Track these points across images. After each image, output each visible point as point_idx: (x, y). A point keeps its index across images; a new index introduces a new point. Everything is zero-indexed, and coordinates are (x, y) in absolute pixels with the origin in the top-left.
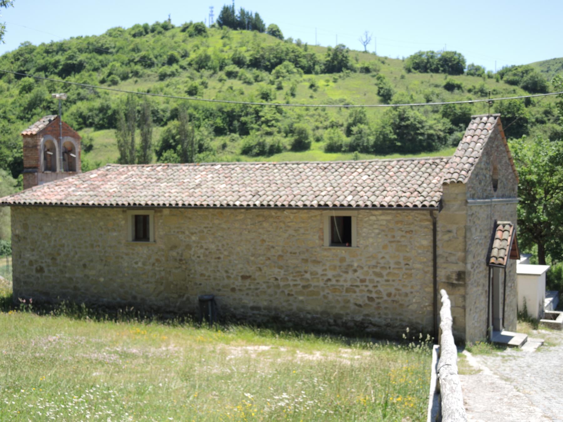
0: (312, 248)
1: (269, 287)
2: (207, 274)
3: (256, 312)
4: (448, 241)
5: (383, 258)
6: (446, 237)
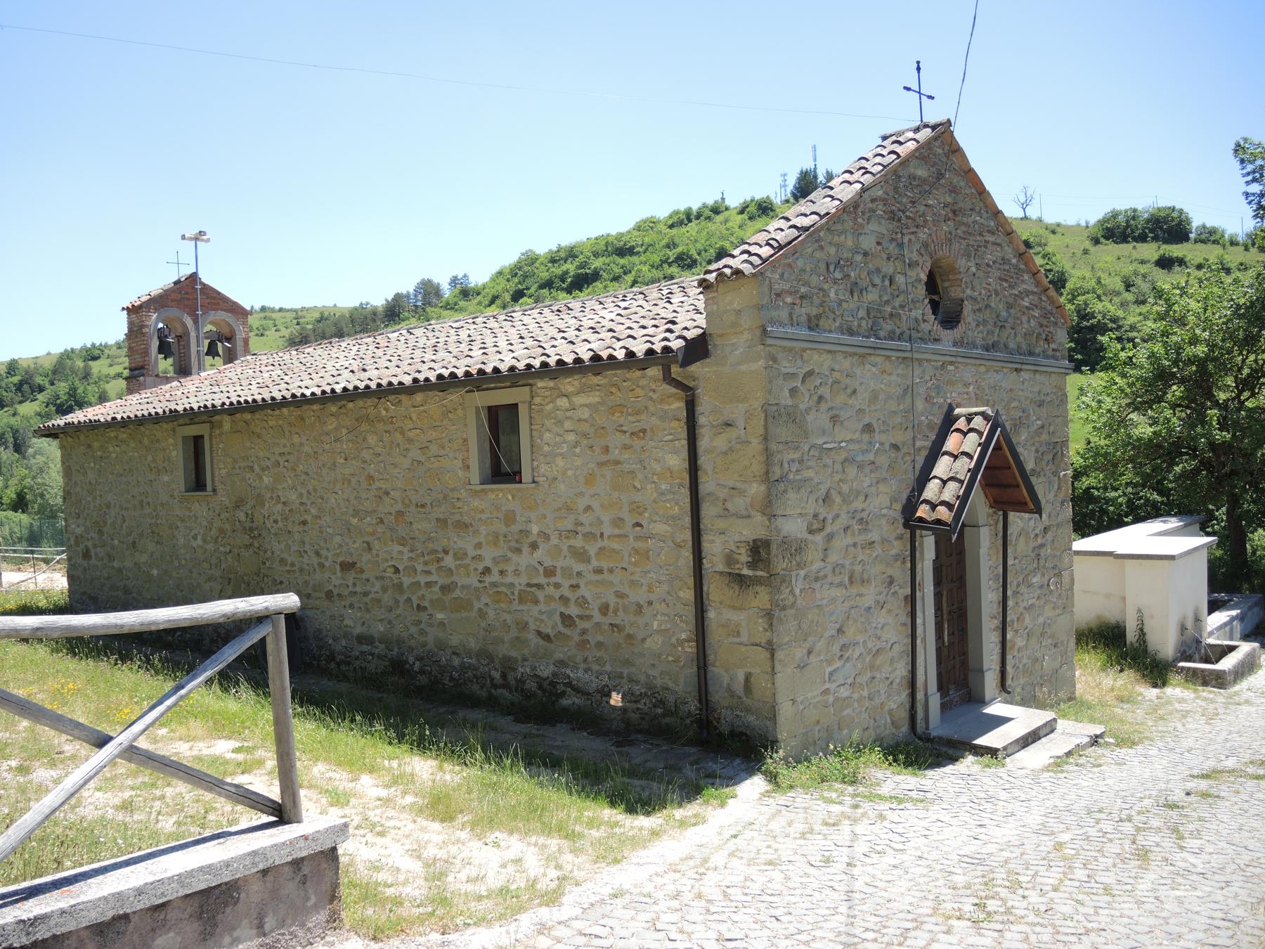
0: (452, 490)
1: (384, 589)
2: (290, 560)
3: (365, 648)
4: (725, 453)
5: (588, 508)
6: (721, 443)
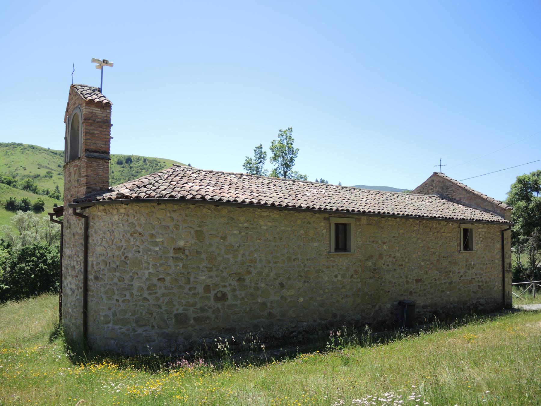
1: (431, 287)
2: (394, 281)
3: (425, 310)
5: (484, 257)
